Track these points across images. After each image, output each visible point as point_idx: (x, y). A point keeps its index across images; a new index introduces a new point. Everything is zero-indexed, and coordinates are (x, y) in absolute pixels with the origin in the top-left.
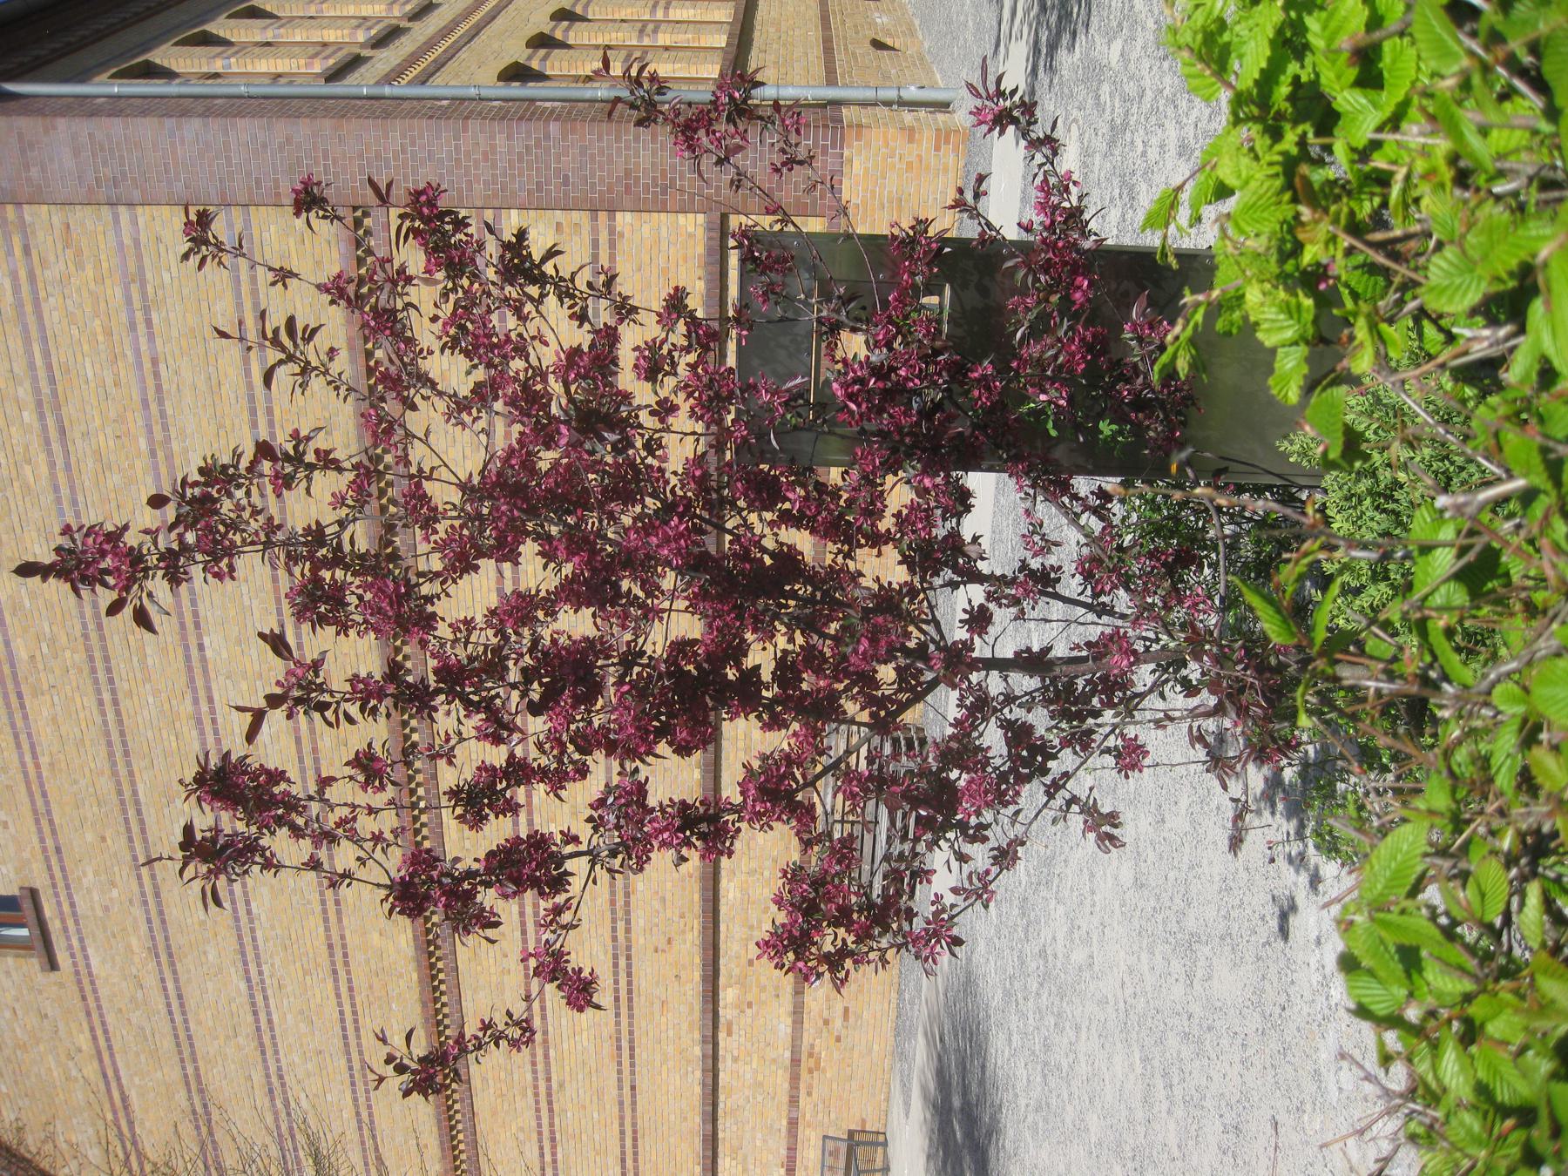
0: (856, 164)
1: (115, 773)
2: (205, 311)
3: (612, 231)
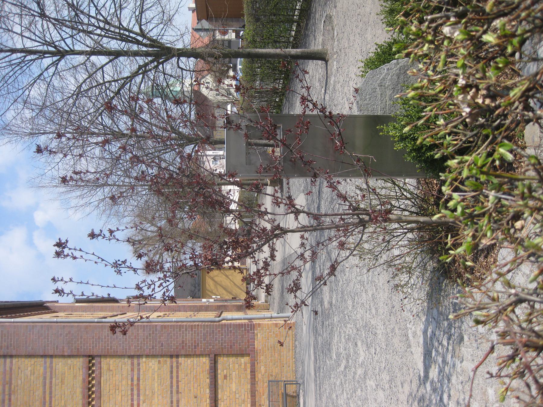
0: (259, 335)
2: (32, 394)
3: (177, 363)
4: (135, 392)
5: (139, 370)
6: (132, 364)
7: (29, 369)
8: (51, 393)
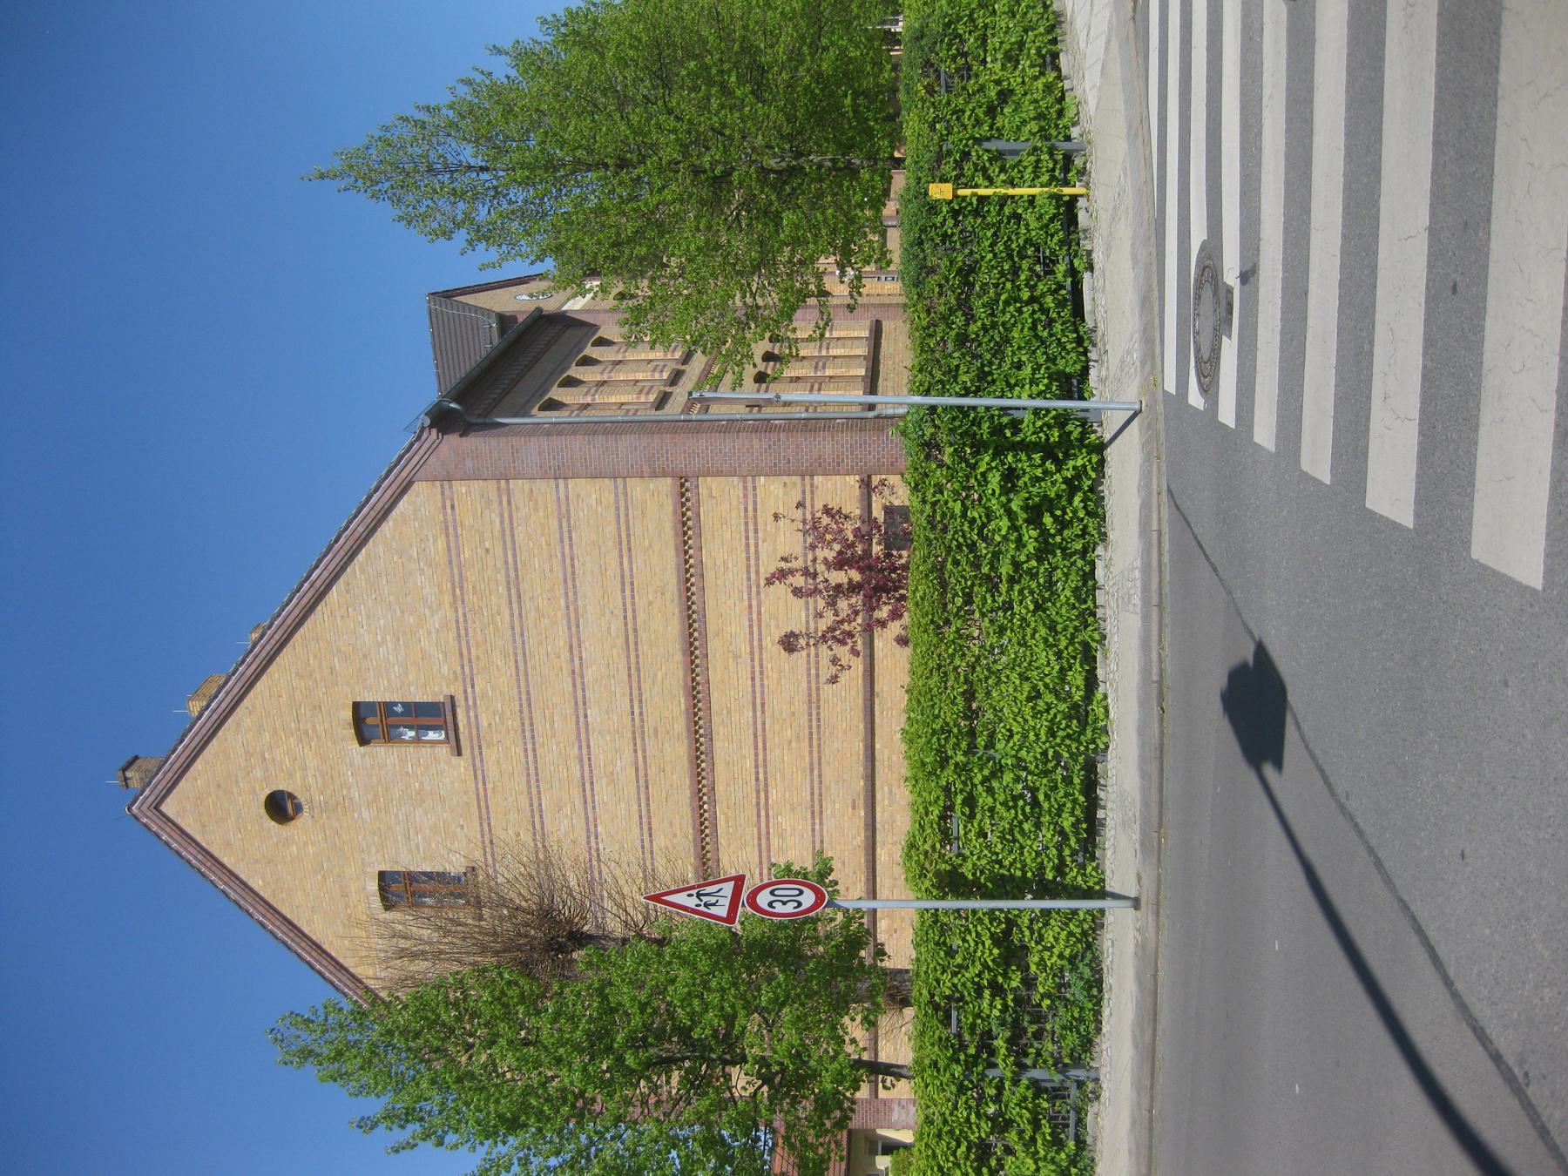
1: (530, 793)
4: (751, 527)
5: (755, 496)
6: (745, 488)
8: (628, 529)
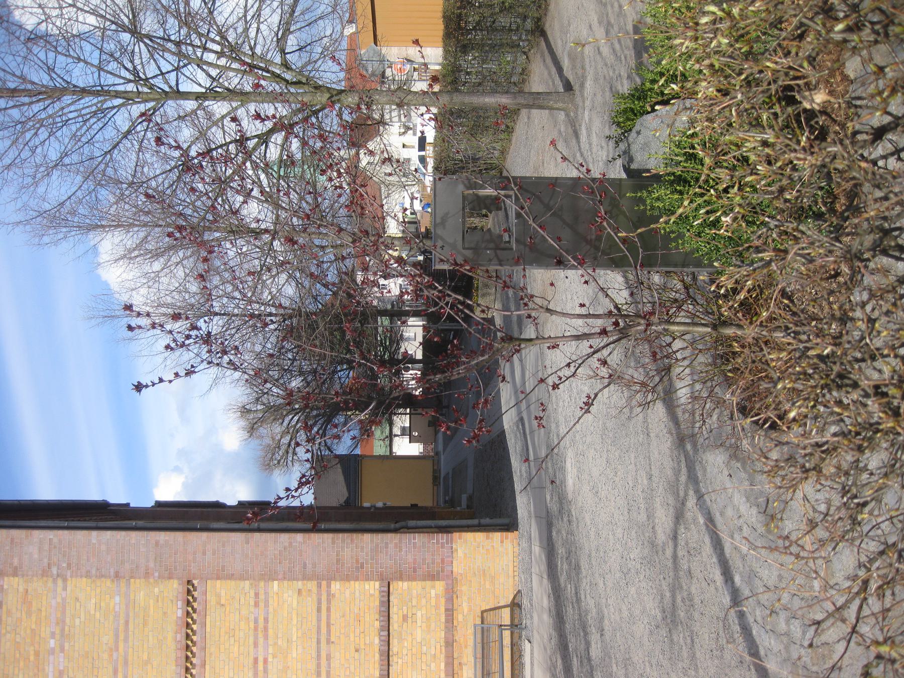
7: (93, 601)
